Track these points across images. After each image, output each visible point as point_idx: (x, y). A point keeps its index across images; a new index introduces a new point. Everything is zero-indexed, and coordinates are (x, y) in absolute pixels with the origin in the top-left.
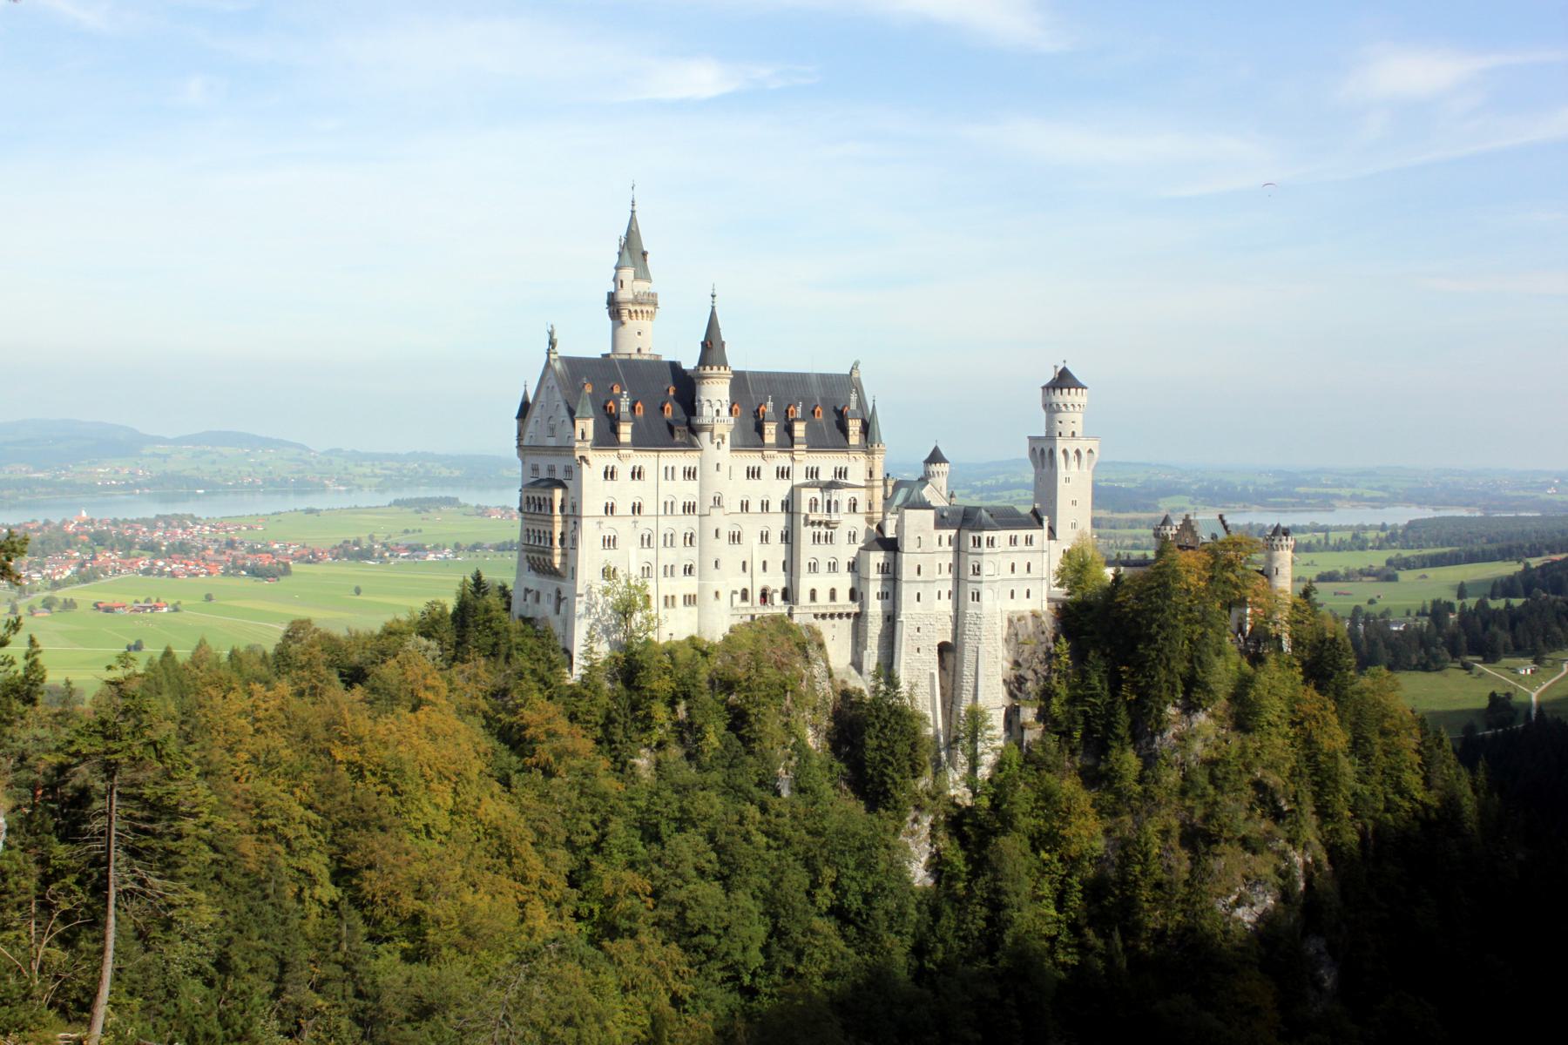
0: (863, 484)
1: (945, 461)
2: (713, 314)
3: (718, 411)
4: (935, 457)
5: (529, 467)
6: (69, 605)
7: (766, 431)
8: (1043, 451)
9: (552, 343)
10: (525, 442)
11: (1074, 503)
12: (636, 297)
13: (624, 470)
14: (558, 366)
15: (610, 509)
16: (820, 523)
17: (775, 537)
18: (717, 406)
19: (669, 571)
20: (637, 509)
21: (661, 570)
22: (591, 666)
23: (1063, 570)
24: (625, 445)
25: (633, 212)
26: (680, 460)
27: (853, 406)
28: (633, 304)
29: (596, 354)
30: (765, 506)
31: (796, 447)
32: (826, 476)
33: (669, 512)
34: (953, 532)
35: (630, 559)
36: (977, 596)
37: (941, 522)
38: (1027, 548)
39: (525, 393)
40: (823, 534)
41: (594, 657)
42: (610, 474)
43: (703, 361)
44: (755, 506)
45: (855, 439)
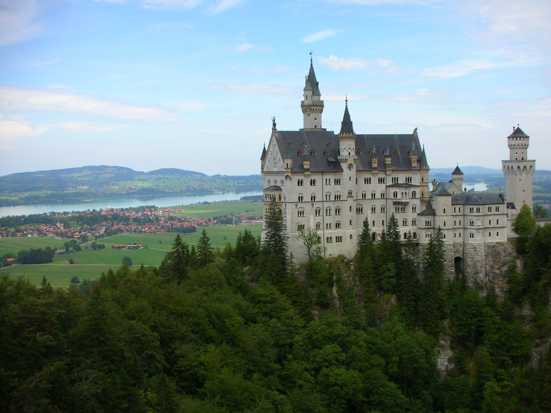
0: (419, 185)
1: (462, 174)
2: (347, 110)
3: (349, 153)
4: (457, 171)
5: (266, 180)
6: (102, 247)
7: (373, 162)
8: (508, 166)
9: (274, 125)
10: (265, 170)
11: (524, 191)
12: (313, 103)
13: (307, 182)
14: (277, 135)
15: (301, 199)
16: (399, 202)
17: (378, 210)
18: (350, 151)
19: (329, 226)
20: (313, 198)
21: (325, 226)
22: (292, 269)
23: (517, 223)
24: (307, 170)
25: (312, 64)
26: (332, 177)
27: (413, 149)
28: (312, 106)
29: (297, 129)
30: (373, 195)
31: (387, 169)
32: (401, 181)
33: (328, 200)
34: (461, 206)
35: (311, 221)
36: (472, 236)
37: (455, 202)
38: (496, 213)
39: (264, 147)
40: (400, 207)
41: (293, 265)
42: (300, 183)
43: (342, 131)
44: (369, 196)
45: (414, 165)
